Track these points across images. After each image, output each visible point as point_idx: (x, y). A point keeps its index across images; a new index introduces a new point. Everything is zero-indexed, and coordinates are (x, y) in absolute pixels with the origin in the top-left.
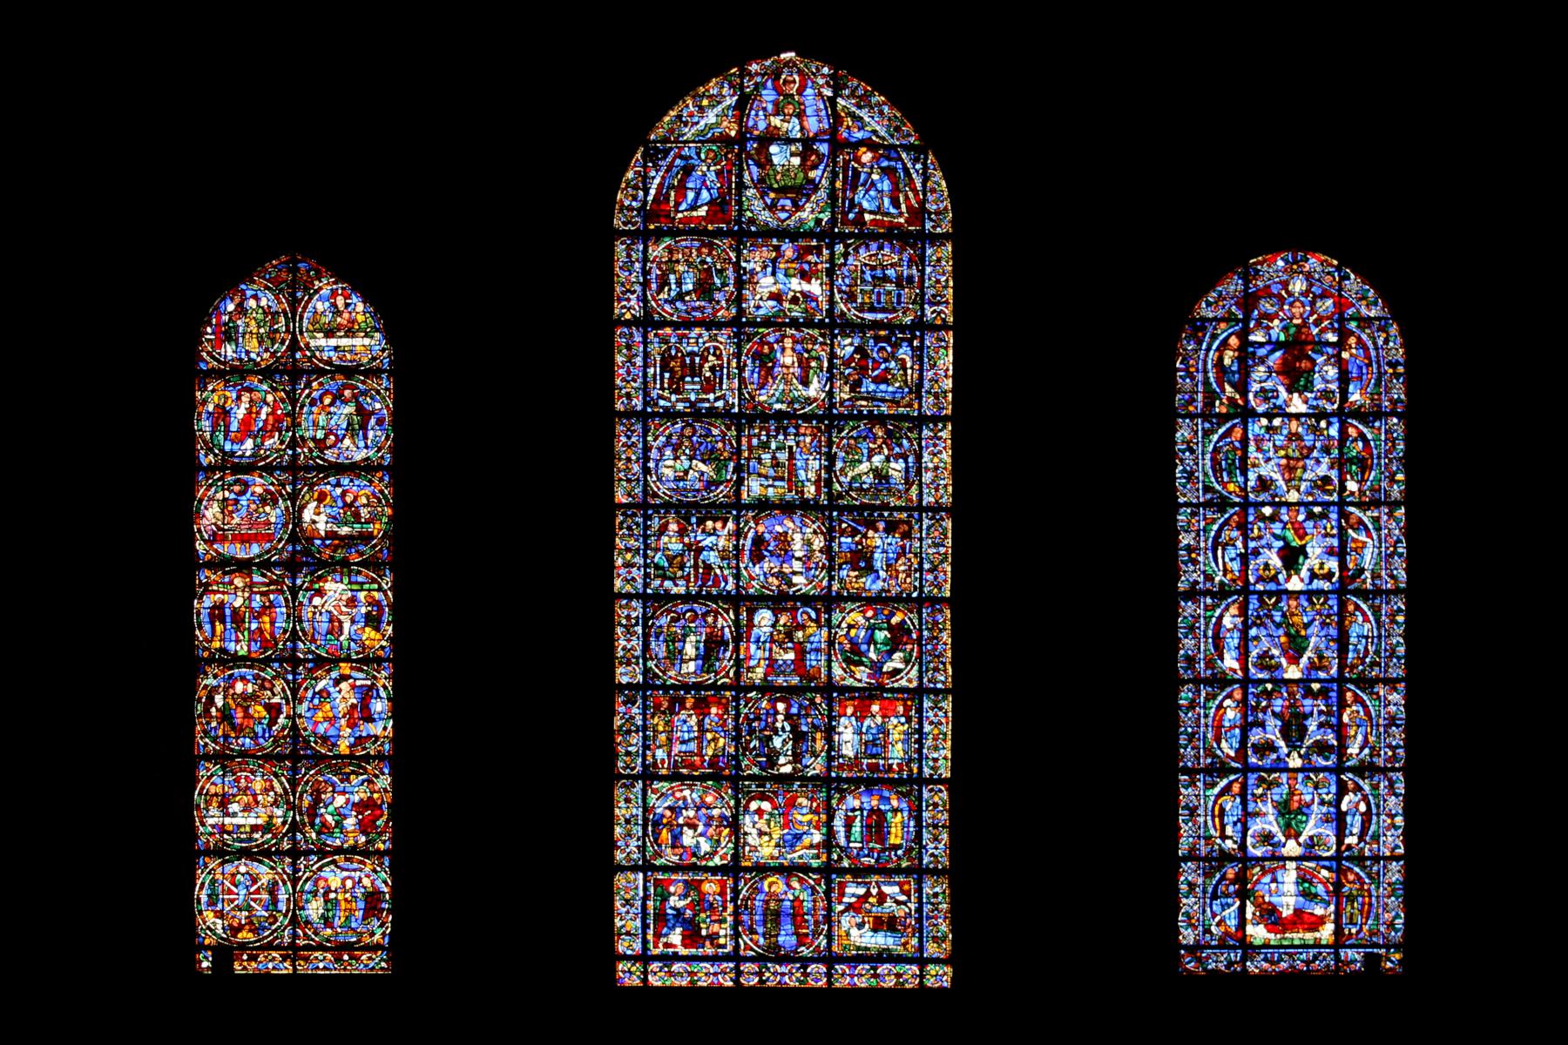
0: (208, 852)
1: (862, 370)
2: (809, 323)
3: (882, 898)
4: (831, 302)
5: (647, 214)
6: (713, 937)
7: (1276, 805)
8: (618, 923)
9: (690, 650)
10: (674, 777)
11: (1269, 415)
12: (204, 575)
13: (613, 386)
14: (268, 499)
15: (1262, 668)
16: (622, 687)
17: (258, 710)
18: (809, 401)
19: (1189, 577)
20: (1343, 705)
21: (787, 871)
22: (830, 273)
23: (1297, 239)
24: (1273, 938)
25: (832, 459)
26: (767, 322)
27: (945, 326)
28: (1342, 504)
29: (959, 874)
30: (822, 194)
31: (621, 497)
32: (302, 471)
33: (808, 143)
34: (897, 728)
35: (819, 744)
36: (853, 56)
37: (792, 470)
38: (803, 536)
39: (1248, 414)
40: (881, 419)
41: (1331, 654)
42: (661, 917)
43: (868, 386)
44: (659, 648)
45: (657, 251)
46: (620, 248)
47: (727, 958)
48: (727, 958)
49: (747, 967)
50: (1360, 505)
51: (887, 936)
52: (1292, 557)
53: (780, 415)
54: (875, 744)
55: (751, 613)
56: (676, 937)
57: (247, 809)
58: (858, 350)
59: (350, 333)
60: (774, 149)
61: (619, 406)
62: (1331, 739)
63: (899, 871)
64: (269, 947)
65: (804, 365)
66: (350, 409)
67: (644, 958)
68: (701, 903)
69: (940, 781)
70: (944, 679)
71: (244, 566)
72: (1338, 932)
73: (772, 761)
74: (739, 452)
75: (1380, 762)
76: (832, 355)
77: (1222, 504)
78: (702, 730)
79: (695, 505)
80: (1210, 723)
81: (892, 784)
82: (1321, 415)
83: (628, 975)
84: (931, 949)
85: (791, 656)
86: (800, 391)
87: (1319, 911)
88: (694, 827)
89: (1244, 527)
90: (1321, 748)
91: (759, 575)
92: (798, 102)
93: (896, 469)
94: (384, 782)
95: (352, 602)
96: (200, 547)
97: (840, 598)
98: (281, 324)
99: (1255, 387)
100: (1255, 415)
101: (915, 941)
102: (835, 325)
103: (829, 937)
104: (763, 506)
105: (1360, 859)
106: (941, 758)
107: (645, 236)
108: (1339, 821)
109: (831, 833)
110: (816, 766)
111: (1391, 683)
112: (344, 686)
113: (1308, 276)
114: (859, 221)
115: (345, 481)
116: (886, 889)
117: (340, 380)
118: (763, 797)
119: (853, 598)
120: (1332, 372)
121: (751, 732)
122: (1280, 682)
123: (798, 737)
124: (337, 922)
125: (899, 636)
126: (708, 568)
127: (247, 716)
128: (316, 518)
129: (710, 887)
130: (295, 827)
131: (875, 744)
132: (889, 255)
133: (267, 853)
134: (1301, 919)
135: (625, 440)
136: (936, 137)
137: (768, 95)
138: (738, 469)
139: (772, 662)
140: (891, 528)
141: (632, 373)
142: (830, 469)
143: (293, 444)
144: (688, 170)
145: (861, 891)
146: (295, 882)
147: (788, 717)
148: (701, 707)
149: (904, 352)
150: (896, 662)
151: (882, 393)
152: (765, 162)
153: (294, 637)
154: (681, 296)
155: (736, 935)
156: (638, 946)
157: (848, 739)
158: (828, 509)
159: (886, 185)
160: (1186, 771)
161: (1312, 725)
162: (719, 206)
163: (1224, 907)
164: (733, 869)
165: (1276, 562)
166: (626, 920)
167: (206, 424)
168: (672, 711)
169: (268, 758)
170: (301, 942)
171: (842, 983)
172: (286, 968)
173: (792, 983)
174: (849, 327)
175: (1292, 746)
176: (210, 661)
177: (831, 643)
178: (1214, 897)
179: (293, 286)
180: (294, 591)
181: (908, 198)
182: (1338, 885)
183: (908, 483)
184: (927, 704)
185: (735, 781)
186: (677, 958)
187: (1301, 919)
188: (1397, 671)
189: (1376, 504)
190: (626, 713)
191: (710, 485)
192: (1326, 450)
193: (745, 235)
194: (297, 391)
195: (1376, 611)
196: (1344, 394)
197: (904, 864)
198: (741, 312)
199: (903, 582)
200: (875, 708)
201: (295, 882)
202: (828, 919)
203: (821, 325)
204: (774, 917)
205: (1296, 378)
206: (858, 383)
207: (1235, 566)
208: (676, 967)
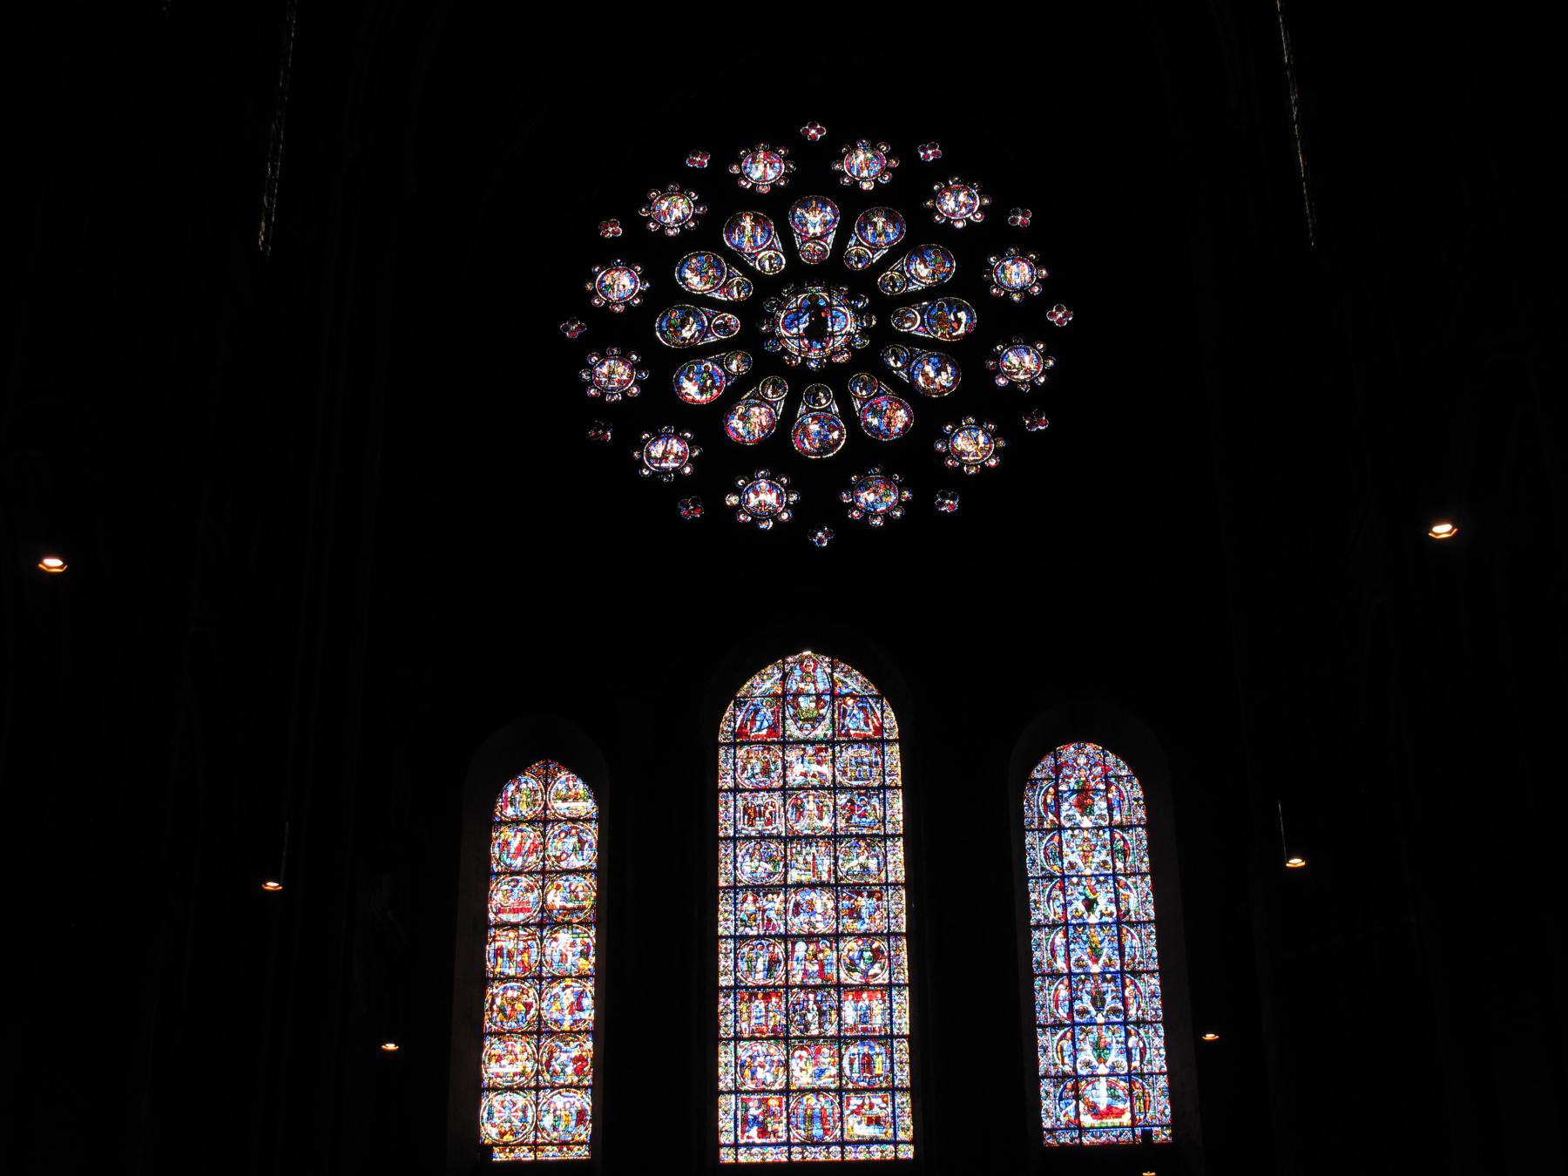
0: (489, 1089)
1: (852, 811)
2: (822, 787)
3: (871, 1106)
4: (834, 776)
5: (736, 735)
6: (775, 1132)
7: (1092, 1044)
8: (721, 1124)
9: (760, 966)
11: (1072, 829)
12: (492, 932)
13: (717, 824)
14: (529, 889)
15: (1079, 966)
16: (722, 988)
17: (520, 1007)
18: (823, 828)
19: (1036, 917)
20: (1124, 986)
21: (817, 1091)
22: (833, 761)
23: (1080, 736)
24: (1096, 1123)
25: (836, 859)
26: (800, 788)
27: (897, 787)
28: (1114, 875)
29: (917, 1090)
30: (827, 721)
31: (722, 883)
32: (547, 874)
33: (819, 696)
34: (878, 1007)
35: (834, 1017)
36: (839, 650)
37: (815, 866)
39: (1061, 829)
40: (863, 837)
41: (1116, 958)
42: (745, 1121)
43: (855, 819)
44: (743, 966)
45: (741, 753)
46: (722, 752)
47: (783, 1144)
48: (783, 1144)
49: (795, 1149)
50: (1125, 875)
52: (1090, 904)
53: (807, 837)
54: (865, 1017)
55: (794, 944)
56: (754, 1132)
58: (850, 800)
59: (576, 799)
60: (801, 699)
61: (721, 834)
62: (1120, 1006)
63: (881, 1089)
64: (521, 1144)
65: (820, 809)
66: (575, 839)
67: (736, 1145)
68: (768, 1112)
69: (903, 1036)
70: (904, 977)
72: (1133, 1118)
73: (807, 1029)
74: (785, 857)
75: (1148, 1018)
76: (835, 804)
77: (1051, 877)
78: (767, 1011)
79: (762, 886)
80: (1051, 998)
82: (1100, 828)
83: (727, 1156)
84: (901, 1136)
85: (816, 968)
86: (819, 823)
87: (1120, 1106)
88: (762, 1066)
89: (1063, 890)
90: (1115, 1011)
91: (798, 924)
92: (813, 674)
93: (872, 864)
94: (589, 1045)
95: (573, 944)
96: (491, 916)
97: (843, 935)
98: (539, 796)
99: (1063, 814)
101: (891, 1131)
102: (836, 788)
103: (842, 1130)
104: (799, 885)
105: (1142, 1075)
106: (903, 1024)
107: (734, 745)
108: (1129, 1053)
109: (841, 1069)
110: (832, 1030)
111: (1150, 973)
112: (568, 991)
113: (1087, 755)
114: (847, 734)
115: (571, 878)
116: (874, 1101)
117: (570, 825)
118: (802, 1048)
119: (850, 935)
120: (1104, 805)
121: (795, 1011)
122: (1088, 974)
123: (822, 1013)
125: (877, 954)
126: (770, 920)
127: (513, 1009)
128: (555, 899)
129: (773, 1102)
130: (538, 1073)
131: (865, 1017)
132: (864, 751)
133: (521, 1089)
134: (1110, 1111)
135: (725, 851)
136: (888, 689)
137: (798, 672)
138: (785, 866)
139: (806, 972)
140: (870, 895)
141: (729, 815)
142: (836, 864)
143: (544, 859)
144: (757, 712)
145: (860, 1102)
146: (537, 1105)
147: (816, 1002)
148: (767, 998)
149: (875, 801)
150: (876, 969)
151: (863, 824)
152: (797, 706)
153: (541, 964)
154: (753, 776)
155: (788, 1130)
156: (732, 1138)
157: (850, 1014)
158: (835, 886)
159: (861, 715)
160: (1040, 1026)
161: (1108, 998)
162: (772, 729)
163: (1067, 1104)
164: (786, 1091)
165: (1082, 908)
166: (725, 1123)
167: (497, 850)
168: (750, 1000)
169: (524, 1033)
171: (849, 1157)
172: (531, 1156)
173: (821, 1158)
175: (1098, 1010)
176: (494, 979)
177: (839, 960)
178: (1061, 1099)
179: (546, 776)
180: (542, 939)
182: (1131, 1090)
183: (880, 870)
184: (894, 992)
185: (786, 1039)
186: (754, 1145)
187: (1110, 1111)
188: (1154, 966)
189: (1134, 874)
190: (725, 1003)
191: (770, 875)
192: (1104, 847)
193: (785, 744)
194: (546, 839)
195: (1139, 934)
196: (1111, 816)
198: (785, 783)
199: (878, 924)
200: (865, 995)
201: (537, 1105)
202: (841, 1119)
203: (828, 788)
204: (810, 1119)
205: (1084, 807)
206: (850, 818)
207: (1060, 910)
208: (755, 1150)
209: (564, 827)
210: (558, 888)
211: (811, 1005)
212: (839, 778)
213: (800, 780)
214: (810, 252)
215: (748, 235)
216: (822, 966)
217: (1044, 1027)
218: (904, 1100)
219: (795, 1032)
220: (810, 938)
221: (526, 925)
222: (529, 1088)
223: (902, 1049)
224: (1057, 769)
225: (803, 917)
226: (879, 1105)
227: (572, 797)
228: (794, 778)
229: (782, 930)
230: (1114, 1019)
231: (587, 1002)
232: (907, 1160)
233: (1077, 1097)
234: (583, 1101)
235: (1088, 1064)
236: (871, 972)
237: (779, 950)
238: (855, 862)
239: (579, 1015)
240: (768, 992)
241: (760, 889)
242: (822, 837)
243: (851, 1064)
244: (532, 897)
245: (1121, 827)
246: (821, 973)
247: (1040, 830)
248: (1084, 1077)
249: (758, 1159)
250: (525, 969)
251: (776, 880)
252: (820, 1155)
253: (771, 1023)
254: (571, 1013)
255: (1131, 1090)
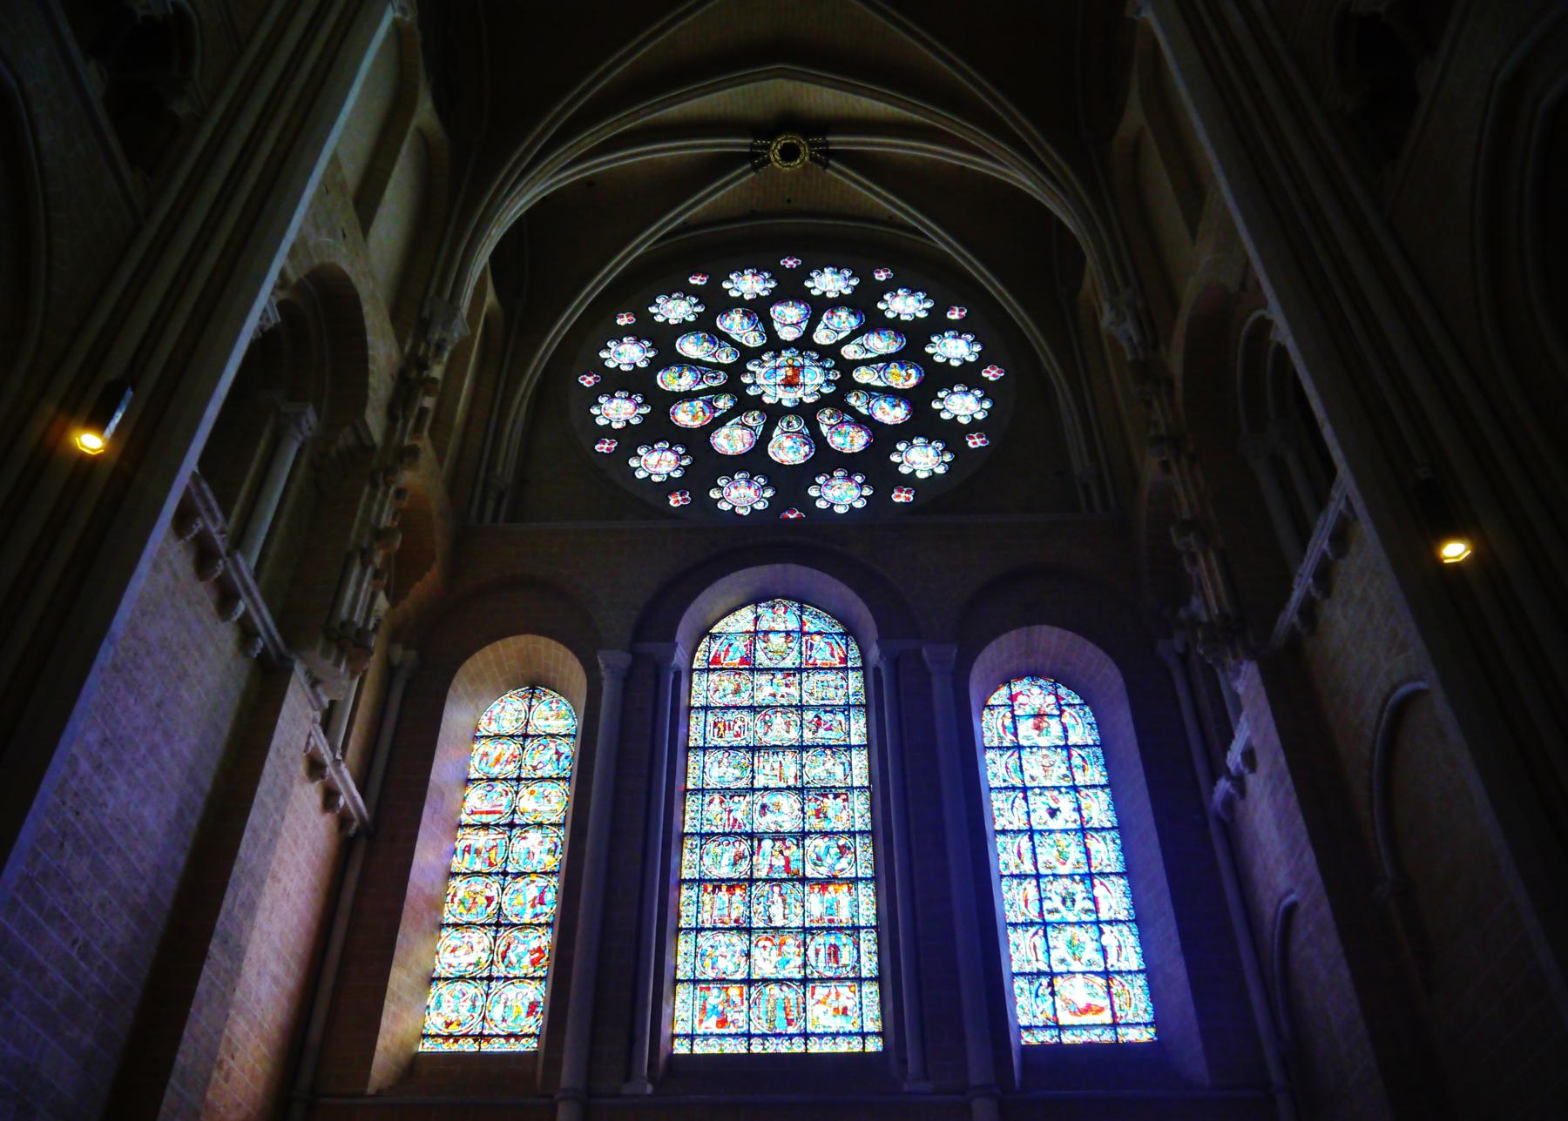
1: (818, 725)
3: (838, 995)
10: (714, 929)
17: (482, 900)
20: (1093, 886)
21: (780, 982)
30: (795, 653)
33: (788, 633)
38: (789, 803)
40: (830, 747)
41: (1083, 859)
42: (704, 1009)
46: (695, 677)
48: (743, 1035)
51: (844, 1017)
52: (1053, 813)
55: (760, 841)
56: (711, 1025)
57: (467, 954)
62: (1091, 905)
63: (847, 978)
64: (466, 1036)
65: (788, 724)
71: (486, 826)
72: (1114, 1015)
75: (1121, 917)
81: (840, 929)
83: (681, 1048)
85: (783, 863)
89: (1025, 798)
90: (1087, 911)
91: (763, 823)
97: (810, 833)
100: (1023, 747)
104: (766, 789)
105: (1120, 973)
107: (708, 670)
110: (797, 922)
124: (509, 1020)
125: (843, 850)
127: (475, 902)
132: (830, 676)
133: (474, 979)
141: (697, 729)
148: (731, 890)
150: (843, 863)
158: (801, 790)
159: (828, 649)
161: (1078, 898)
162: (743, 660)
164: (749, 982)
167: (477, 758)
169: (482, 925)
170: (486, 1032)
174: (809, 707)
181: (838, 653)
182: (1109, 987)
183: (846, 776)
189: (1094, 786)
196: (1066, 738)
197: (851, 975)
207: (1025, 817)
208: (712, 1041)
209: (543, 741)
210: (532, 793)
211: (776, 897)
212: (805, 697)
213: (769, 701)
214: (787, 334)
215: (735, 324)
216: (787, 860)
217: (1015, 925)
218: (870, 990)
219: (757, 922)
220: (778, 836)
221: (497, 825)
222: (481, 979)
223: (868, 942)
224: (1013, 698)
225: (770, 817)
226: (846, 995)
227: (555, 716)
228: (762, 697)
229: (748, 829)
230: (1086, 918)
231: (550, 897)
232: (877, 1053)
233: (1053, 994)
234: (536, 992)
235: (1063, 961)
236: (838, 867)
237: (744, 847)
238: (820, 769)
239: (539, 909)
240: (732, 884)
241: (727, 793)
242: (790, 747)
243: (817, 954)
244: (505, 801)
245: (1075, 746)
246: (787, 868)
247: (1000, 748)
248: (1061, 974)
249: (715, 1051)
250: (491, 865)
251: (743, 784)
252: (783, 1047)
253: (734, 917)
254: (533, 906)
255: (1109, 987)
